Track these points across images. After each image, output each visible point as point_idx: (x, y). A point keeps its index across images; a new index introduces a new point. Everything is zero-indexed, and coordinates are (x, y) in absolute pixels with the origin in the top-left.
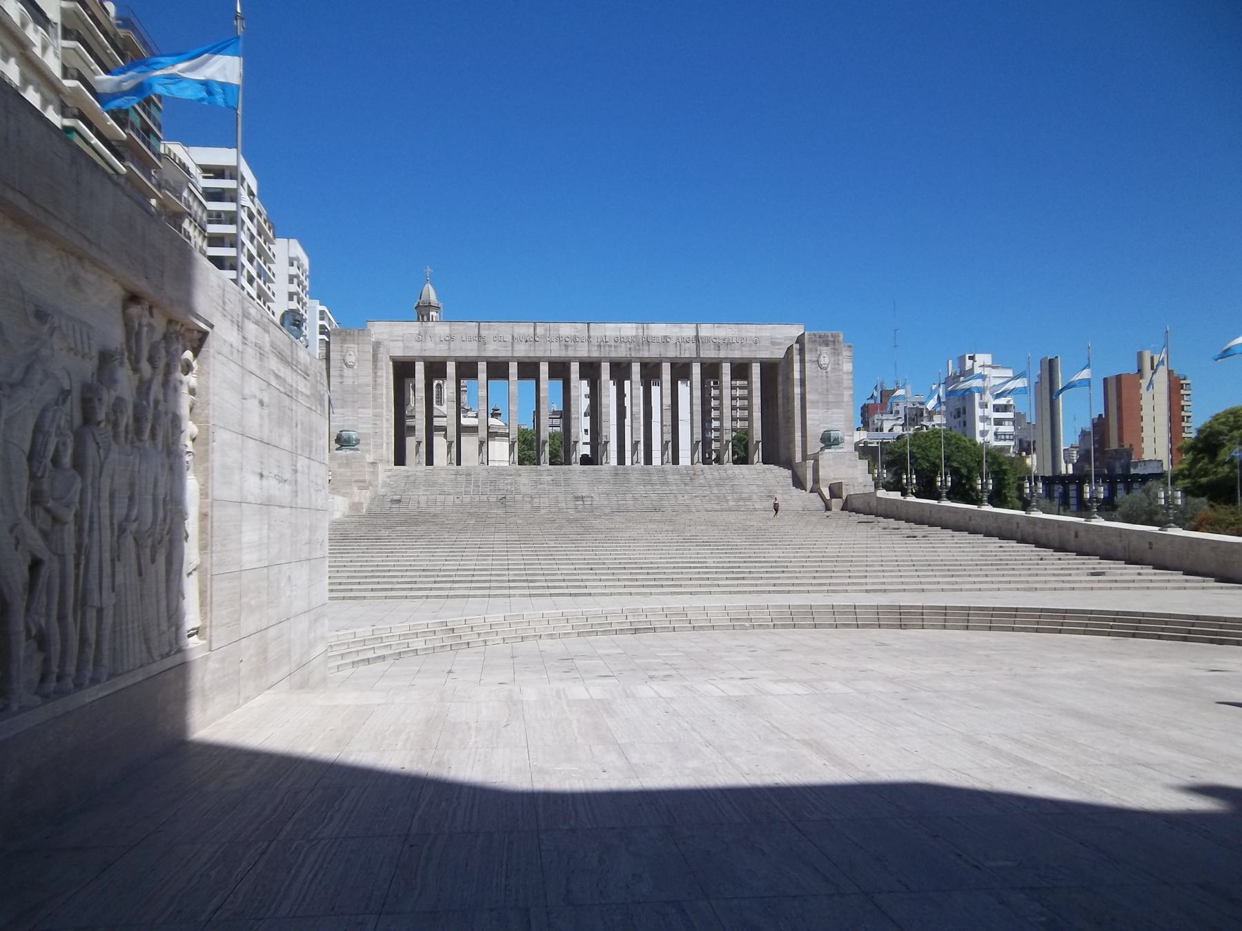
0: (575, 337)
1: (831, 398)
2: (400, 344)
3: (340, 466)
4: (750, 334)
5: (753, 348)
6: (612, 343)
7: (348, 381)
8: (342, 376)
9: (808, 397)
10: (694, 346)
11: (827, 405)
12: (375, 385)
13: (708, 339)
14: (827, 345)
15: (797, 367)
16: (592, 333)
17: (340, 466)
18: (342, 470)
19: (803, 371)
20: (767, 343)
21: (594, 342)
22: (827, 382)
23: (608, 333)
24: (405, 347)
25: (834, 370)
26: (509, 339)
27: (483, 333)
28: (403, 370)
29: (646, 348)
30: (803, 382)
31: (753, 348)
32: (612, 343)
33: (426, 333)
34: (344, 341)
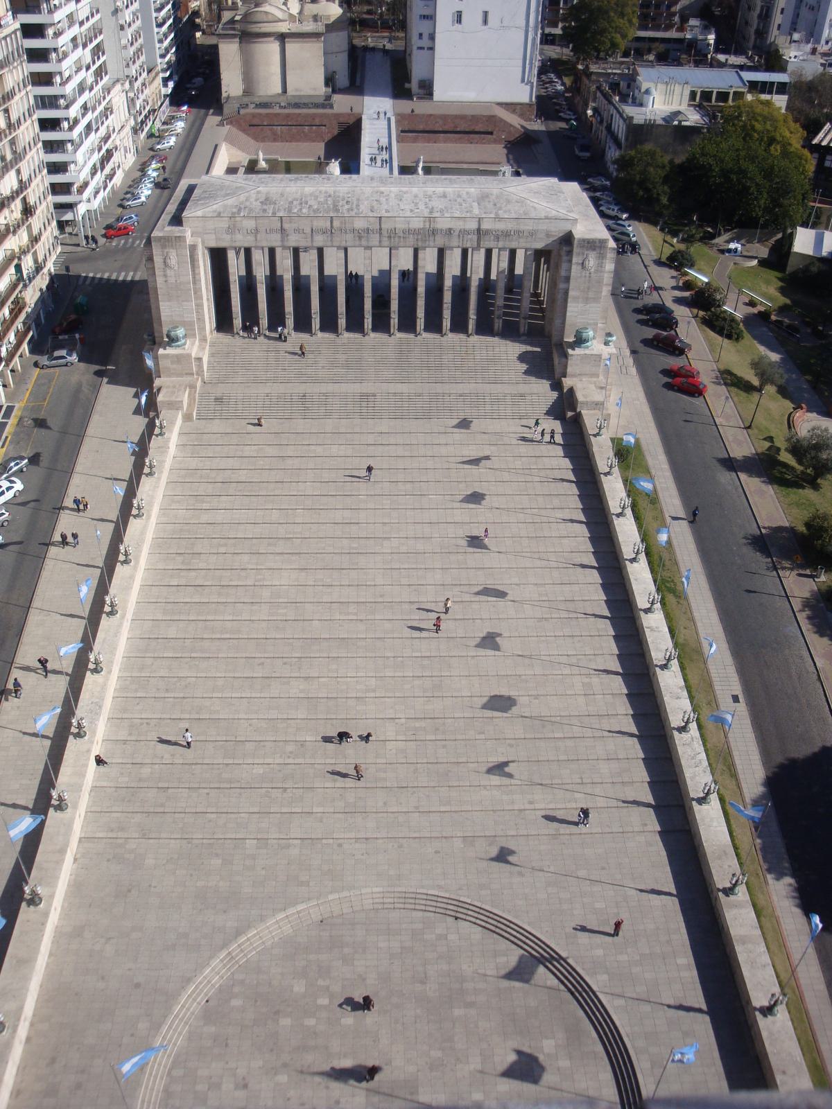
0: (368, 229)
1: (591, 295)
2: (214, 236)
3: (172, 363)
4: (527, 228)
5: (529, 239)
6: (402, 235)
7: (172, 280)
8: (165, 276)
9: (571, 293)
10: (475, 237)
11: (587, 300)
12: (196, 280)
13: (487, 232)
14: (594, 250)
15: (564, 266)
16: (383, 226)
17: (172, 363)
18: (174, 366)
19: (570, 270)
20: (542, 235)
21: (385, 233)
22: (589, 281)
23: (398, 226)
24: (217, 239)
25: (596, 271)
26: (308, 230)
27: (286, 226)
28: (218, 257)
29: (432, 238)
30: (567, 279)
31: (529, 239)
32: (402, 235)
33: (234, 225)
34: (164, 247)
